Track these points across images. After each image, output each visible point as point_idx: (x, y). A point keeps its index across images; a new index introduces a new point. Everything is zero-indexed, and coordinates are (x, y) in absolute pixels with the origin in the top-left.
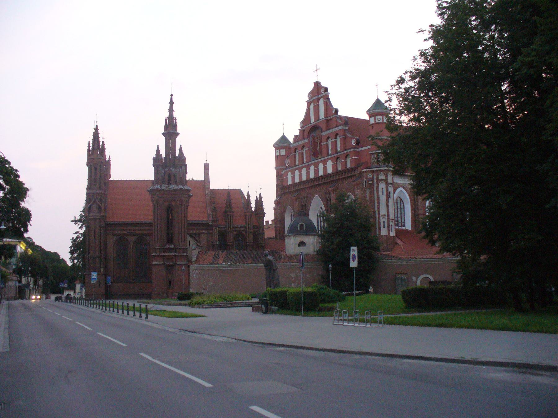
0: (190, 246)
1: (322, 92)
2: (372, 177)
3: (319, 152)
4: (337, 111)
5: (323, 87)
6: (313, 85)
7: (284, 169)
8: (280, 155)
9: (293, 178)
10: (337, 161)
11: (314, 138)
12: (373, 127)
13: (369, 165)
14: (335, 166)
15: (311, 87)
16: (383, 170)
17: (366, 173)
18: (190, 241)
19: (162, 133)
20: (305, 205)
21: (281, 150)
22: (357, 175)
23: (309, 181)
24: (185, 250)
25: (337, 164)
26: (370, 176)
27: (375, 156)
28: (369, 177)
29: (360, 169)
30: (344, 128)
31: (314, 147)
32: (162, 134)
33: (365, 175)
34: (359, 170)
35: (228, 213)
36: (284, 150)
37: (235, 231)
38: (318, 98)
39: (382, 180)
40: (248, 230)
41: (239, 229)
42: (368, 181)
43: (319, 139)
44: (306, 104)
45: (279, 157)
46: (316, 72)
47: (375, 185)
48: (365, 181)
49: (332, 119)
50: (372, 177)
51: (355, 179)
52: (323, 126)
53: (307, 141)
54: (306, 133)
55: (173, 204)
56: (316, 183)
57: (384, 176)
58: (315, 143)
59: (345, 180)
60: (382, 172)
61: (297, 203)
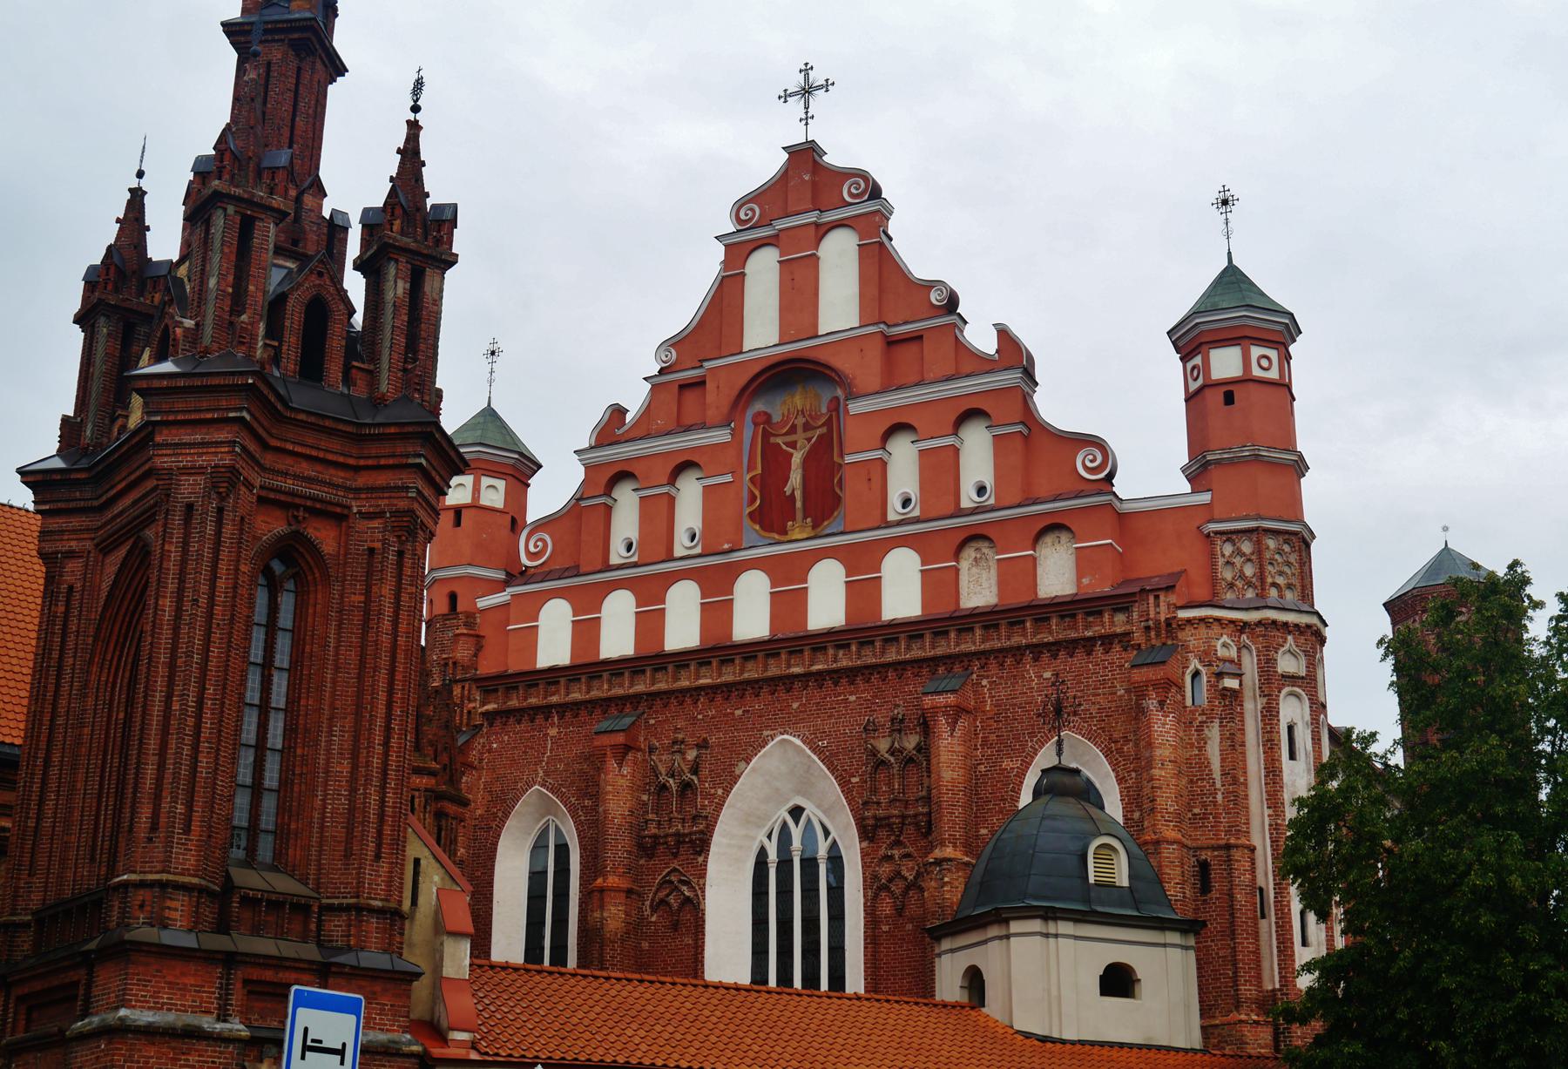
0: (414, 902)
1: (848, 199)
2: (1233, 653)
3: (799, 504)
4: (952, 302)
5: (863, 175)
6: (786, 156)
7: (506, 583)
8: (475, 506)
9: (586, 632)
10: (957, 557)
11: (764, 420)
12: (1229, 399)
13: (1202, 593)
14: (938, 584)
15: (768, 164)
16: (1296, 625)
17: (1203, 631)
19: (226, 18)
20: (686, 786)
21: (486, 481)
22: (1138, 637)
24: (395, 918)
25: (957, 570)
26: (1225, 647)
27: (1247, 547)
28: (1221, 652)
29: (1163, 608)
30: (1023, 386)
32: (223, 24)
33: (1190, 637)
34: (1161, 610)
36: (501, 484)
38: (817, 225)
39: (1292, 679)
42: (1220, 675)
43: (800, 437)
44: (719, 252)
45: (464, 512)
46: (796, 105)
47: (1252, 708)
48: (1196, 674)
49: (920, 338)
50: (1233, 653)
51: (1116, 653)
52: (863, 368)
53: (721, 436)
54: (717, 398)
55: (325, 537)
56: (789, 666)
57: (1303, 661)
58: (775, 463)
59: (1036, 659)
60: (1290, 638)
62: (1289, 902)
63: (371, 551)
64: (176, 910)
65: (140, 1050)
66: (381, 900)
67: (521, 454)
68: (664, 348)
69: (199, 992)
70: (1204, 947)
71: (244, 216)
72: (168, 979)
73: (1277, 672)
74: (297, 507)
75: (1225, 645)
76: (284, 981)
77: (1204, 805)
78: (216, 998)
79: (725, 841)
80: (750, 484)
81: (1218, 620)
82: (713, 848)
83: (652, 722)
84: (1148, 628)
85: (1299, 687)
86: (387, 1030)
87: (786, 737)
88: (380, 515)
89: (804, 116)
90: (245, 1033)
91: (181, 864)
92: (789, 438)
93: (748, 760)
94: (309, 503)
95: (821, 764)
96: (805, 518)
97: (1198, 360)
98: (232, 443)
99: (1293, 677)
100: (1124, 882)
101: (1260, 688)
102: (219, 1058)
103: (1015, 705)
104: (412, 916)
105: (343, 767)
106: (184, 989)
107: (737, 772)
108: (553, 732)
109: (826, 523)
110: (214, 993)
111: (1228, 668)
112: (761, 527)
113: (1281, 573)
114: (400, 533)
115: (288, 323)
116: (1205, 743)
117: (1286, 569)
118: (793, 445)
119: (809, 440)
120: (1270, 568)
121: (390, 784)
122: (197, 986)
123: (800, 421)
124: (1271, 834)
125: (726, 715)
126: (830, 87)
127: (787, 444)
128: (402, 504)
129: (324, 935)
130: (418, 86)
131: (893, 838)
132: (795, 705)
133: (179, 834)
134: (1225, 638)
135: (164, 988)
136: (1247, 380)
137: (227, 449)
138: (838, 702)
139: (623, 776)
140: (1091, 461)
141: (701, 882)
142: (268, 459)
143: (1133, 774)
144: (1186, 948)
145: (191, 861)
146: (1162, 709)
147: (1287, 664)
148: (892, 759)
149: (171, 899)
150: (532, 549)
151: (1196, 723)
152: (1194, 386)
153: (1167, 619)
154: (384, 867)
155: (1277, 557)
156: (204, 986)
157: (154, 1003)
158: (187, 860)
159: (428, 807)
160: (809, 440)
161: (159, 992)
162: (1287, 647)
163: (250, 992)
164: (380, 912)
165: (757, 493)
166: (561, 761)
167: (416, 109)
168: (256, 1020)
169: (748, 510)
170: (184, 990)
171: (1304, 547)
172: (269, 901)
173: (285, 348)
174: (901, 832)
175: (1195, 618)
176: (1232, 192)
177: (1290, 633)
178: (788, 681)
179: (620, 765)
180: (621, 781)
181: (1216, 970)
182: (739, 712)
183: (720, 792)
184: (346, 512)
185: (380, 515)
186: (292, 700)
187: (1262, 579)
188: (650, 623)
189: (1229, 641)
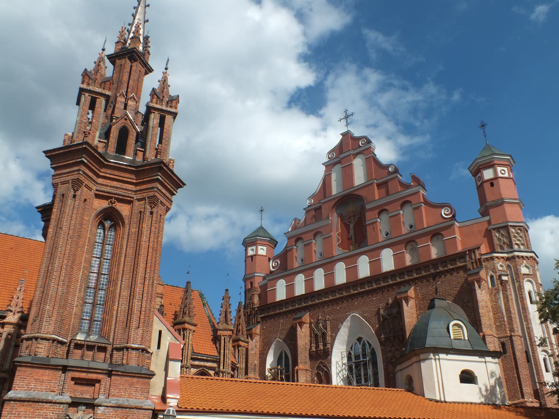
0: (159, 347)
9: (290, 288)
12: (492, 185)
14: (398, 258)
16: (527, 257)
18: (160, 332)
21: (260, 247)
22: (470, 266)
23: (331, 289)
31: (341, 233)
35: (187, 326)
36: (265, 248)
37: (193, 366)
40: (222, 367)
41: (202, 363)
44: (324, 168)
50: (505, 268)
55: (124, 209)
61: (303, 330)
62: (538, 355)
63: (140, 212)
64: (42, 348)
65: (16, 409)
66: (138, 345)
67: (270, 238)
68: (310, 199)
69: (50, 383)
70: (507, 374)
71: (92, 97)
72: (35, 377)
73: (521, 273)
74: (112, 198)
75: (501, 266)
76: (90, 378)
77: (500, 322)
78: (57, 385)
79: (336, 350)
80: (337, 236)
81: (497, 257)
82: (333, 353)
83: (311, 314)
84: (472, 263)
85: (530, 278)
86: (138, 399)
87: (354, 314)
88: (144, 199)
89: (346, 125)
90: (70, 400)
91: (47, 330)
92: (348, 220)
93: (342, 323)
94: (116, 196)
95: (365, 322)
96: (356, 244)
97: (479, 175)
98: (79, 170)
99: (528, 275)
100: (466, 338)
101: (516, 279)
102: (56, 411)
103: (429, 294)
104: (157, 355)
105: (125, 293)
106: (43, 382)
107: (339, 327)
108: (282, 321)
109: (362, 244)
110: (57, 383)
111: (503, 273)
112: (342, 249)
113: (519, 240)
114: (151, 205)
115: (111, 135)
116: (498, 300)
117: (520, 238)
118: (350, 222)
119: (355, 220)
120: (514, 238)
121: (144, 298)
122: (49, 380)
123: (352, 214)
124: (527, 331)
125: (334, 309)
126: (353, 115)
127: (348, 222)
128: (151, 194)
129: (114, 360)
130: (168, 60)
131: (391, 344)
132: (356, 304)
133: (46, 317)
134: (500, 263)
135: (33, 381)
136: (496, 178)
137: (77, 173)
138: (370, 301)
139: (303, 332)
140: (447, 212)
141: (330, 365)
142: (100, 180)
143: (473, 314)
144: (495, 363)
145: (51, 328)
146: (480, 289)
147: (524, 270)
148: (389, 318)
149: (39, 344)
150: (274, 265)
151: (494, 293)
152: (479, 183)
153: (479, 258)
154: (140, 331)
155: (516, 235)
156: (52, 380)
157: (27, 388)
158: (49, 328)
159: (230, 342)
160: (355, 220)
161: (30, 383)
162: (524, 264)
163: (75, 384)
164: (137, 349)
165: (340, 238)
166: (284, 330)
167: (166, 69)
168: (78, 395)
169: (337, 244)
170: (43, 382)
171: (525, 231)
172: (88, 346)
173: (110, 143)
174: (394, 342)
175: (489, 257)
176: (484, 122)
177: (524, 259)
178: (352, 297)
179: (301, 329)
180: (302, 334)
181: (513, 382)
182: (338, 308)
183: (334, 334)
184: (132, 199)
185: (144, 199)
186: (110, 270)
187: (511, 241)
188: (309, 282)
189: (502, 264)
